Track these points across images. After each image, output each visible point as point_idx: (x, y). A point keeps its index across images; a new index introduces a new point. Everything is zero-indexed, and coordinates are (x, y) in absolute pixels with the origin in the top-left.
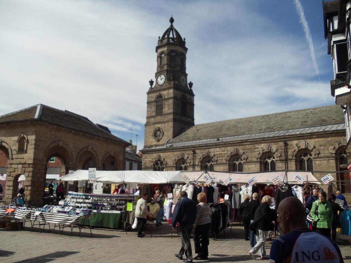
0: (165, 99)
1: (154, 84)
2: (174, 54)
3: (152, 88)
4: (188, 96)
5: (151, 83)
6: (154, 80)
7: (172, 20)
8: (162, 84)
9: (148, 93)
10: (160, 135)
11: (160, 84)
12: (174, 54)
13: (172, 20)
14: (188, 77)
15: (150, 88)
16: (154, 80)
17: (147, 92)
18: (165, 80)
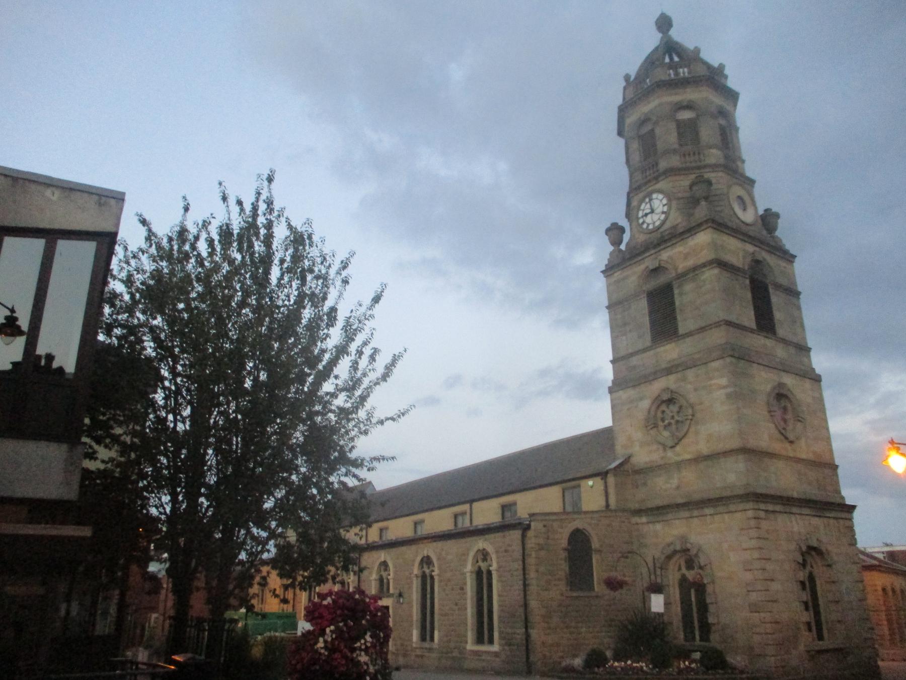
0: (682, 276)
1: (626, 237)
2: (686, 115)
3: (620, 251)
4: (771, 260)
5: (615, 232)
6: (624, 223)
7: (664, 24)
8: (657, 223)
9: (608, 271)
10: (677, 422)
11: (651, 227)
12: (686, 115)
13: (664, 24)
14: (757, 191)
15: (611, 254)
16: (624, 223)
17: (603, 268)
18: (670, 208)
